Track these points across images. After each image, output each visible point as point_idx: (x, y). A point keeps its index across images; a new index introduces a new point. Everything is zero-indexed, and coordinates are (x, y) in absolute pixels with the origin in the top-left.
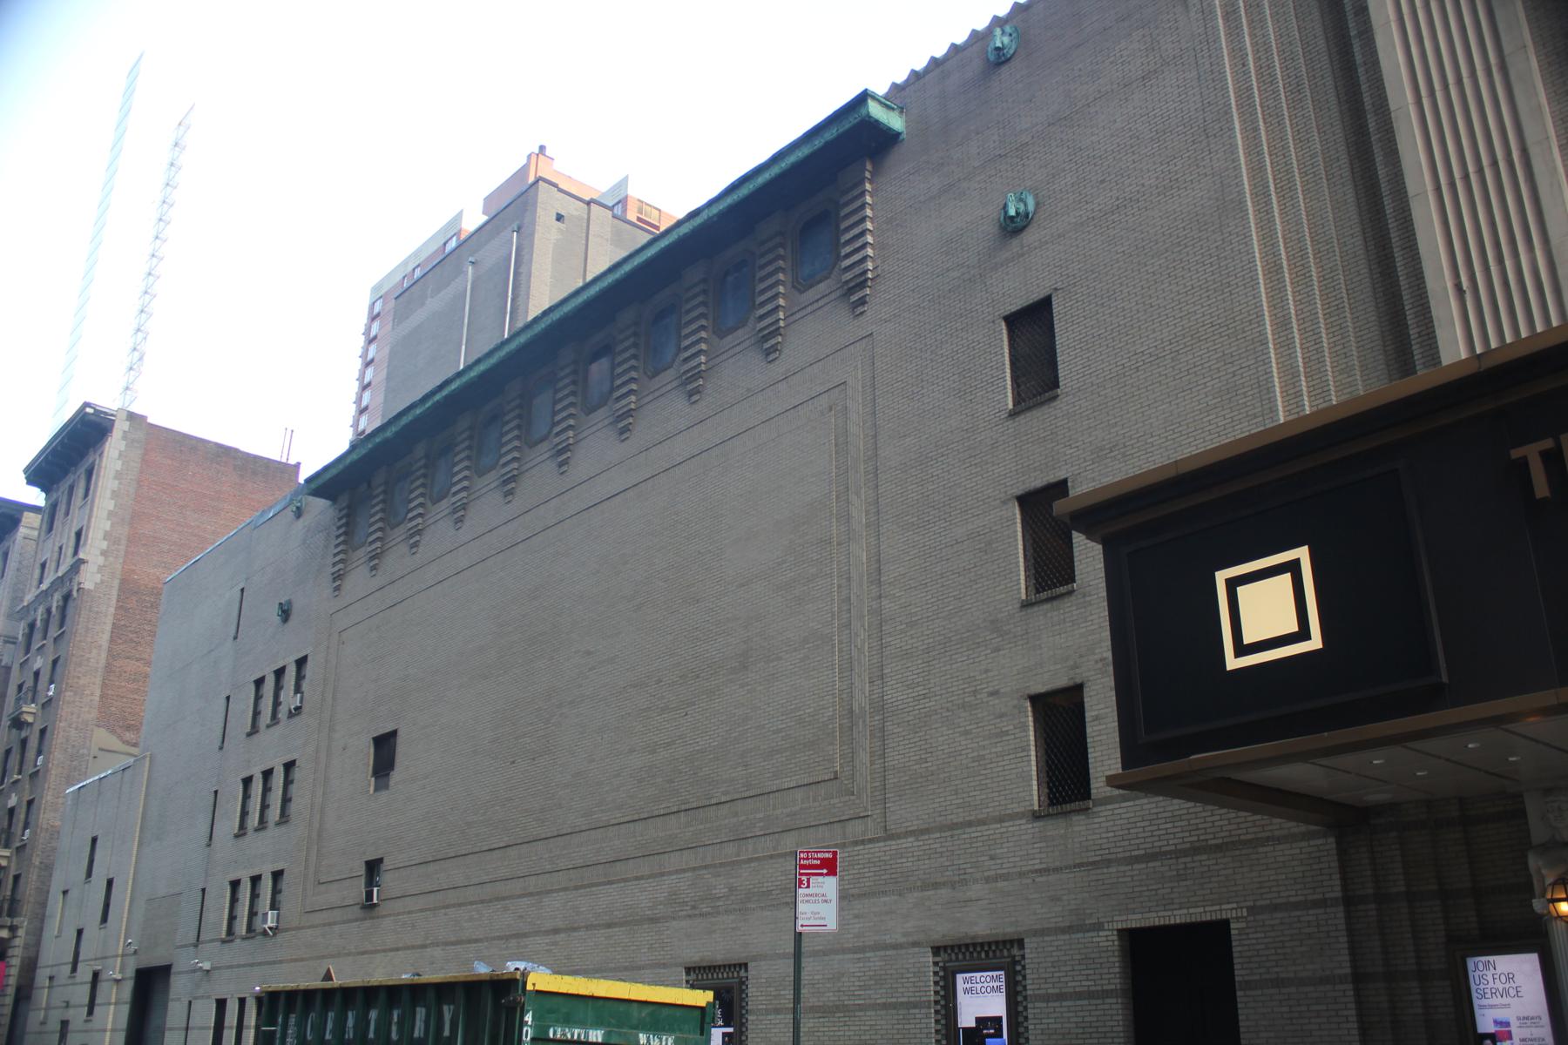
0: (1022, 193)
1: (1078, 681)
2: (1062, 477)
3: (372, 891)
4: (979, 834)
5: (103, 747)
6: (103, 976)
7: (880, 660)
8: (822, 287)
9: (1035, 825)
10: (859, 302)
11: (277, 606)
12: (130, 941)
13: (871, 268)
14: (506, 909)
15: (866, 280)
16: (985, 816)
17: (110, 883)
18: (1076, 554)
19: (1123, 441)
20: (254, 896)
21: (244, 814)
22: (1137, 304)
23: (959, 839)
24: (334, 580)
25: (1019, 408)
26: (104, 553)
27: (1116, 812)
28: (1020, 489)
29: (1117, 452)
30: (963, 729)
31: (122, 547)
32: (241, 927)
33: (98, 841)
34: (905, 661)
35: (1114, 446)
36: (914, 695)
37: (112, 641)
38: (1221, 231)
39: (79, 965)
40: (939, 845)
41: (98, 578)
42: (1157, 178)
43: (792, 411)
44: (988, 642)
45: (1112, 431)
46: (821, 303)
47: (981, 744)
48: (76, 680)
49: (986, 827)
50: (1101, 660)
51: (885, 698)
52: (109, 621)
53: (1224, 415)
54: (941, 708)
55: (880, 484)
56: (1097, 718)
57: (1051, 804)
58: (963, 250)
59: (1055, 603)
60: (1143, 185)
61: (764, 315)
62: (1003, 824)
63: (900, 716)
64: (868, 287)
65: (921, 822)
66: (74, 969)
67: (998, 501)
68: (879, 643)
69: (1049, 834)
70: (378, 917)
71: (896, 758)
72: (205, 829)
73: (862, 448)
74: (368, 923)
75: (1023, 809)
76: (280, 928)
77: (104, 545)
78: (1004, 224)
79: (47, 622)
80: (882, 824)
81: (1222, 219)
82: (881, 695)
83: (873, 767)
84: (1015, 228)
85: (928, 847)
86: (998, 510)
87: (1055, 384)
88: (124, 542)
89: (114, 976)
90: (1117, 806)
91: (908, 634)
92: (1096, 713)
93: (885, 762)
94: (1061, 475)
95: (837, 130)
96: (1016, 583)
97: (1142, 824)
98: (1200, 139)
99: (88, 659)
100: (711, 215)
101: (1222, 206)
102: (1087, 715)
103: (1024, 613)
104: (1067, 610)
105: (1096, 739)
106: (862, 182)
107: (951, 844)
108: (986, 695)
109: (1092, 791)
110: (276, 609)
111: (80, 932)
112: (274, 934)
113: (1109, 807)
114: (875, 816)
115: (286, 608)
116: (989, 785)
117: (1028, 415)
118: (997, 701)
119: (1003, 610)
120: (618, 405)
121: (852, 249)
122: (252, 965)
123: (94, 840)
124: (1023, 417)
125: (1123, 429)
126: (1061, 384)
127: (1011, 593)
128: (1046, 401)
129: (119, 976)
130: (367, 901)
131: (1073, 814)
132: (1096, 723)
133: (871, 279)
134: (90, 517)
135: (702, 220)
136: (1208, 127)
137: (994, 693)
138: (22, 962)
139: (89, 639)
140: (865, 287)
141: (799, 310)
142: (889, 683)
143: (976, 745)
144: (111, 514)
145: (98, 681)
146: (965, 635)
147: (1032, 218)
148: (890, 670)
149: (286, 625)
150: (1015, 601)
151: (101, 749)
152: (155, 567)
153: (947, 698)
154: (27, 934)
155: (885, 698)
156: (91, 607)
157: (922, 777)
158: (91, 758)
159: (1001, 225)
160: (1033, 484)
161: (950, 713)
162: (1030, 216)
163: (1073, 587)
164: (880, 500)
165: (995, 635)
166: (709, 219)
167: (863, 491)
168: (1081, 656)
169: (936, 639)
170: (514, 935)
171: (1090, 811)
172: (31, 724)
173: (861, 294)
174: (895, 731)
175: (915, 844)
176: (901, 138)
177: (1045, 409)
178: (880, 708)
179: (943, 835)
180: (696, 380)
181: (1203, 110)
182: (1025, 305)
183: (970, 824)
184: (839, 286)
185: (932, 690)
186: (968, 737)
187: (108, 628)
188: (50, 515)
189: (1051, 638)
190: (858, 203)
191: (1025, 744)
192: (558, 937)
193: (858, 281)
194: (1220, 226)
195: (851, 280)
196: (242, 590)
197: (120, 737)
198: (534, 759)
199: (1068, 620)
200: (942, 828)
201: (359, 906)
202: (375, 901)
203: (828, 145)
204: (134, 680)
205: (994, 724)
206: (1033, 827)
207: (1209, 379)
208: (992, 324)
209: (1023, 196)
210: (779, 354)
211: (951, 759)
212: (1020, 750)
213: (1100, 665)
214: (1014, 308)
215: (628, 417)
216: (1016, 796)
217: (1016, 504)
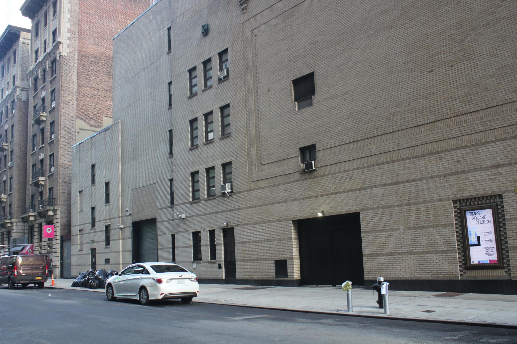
3: (312, 162)
5: (81, 128)
6: (113, 227)
11: (201, 28)
12: (127, 209)
14: (441, 159)
17: (107, 184)
20: (210, 178)
21: (193, 138)
24: (241, 5)
26: (69, 39)
31: (77, 36)
32: (203, 193)
33: (96, 166)
37: (78, 79)
39: (96, 223)
41: (68, 50)
48: (65, 98)
52: (76, 70)
66: (93, 225)
70: (317, 177)
72: (167, 149)
74: (309, 181)
76: (235, 190)
77: (69, 35)
79: (44, 76)
88: (77, 33)
89: (120, 226)
99: (69, 88)
110: (200, 30)
111: (93, 209)
112: (231, 196)
115: (206, 28)
122: (216, 213)
123: (93, 166)
129: (122, 226)
130: (307, 168)
134: (60, 24)
138: (61, 225)
139: (68, 79)
144: (70, 20)
145: (75, 98)
149: (207, 37)
151: (80, 129)
152: (92, 44)
154: (61, 212)
156: (67, 64)
158: (77, 133)
170: (452, 173)
172: (45, 121)
187: (76, 73)
188: (36, 31)
192: (500, 170)
196: (169, 29)
197: (87, 123)
198: (452, 66)
201: (298, 173)
202: (314, 168)
204: (90, 97)
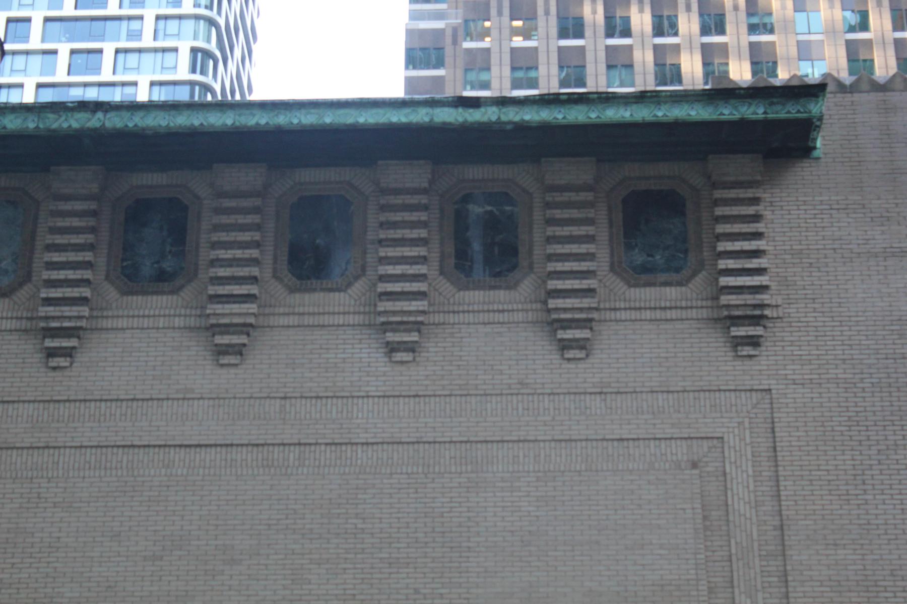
8: (672, 293)
15: (762, 317)
43: (616, 443)
46: (669, 314)
61: (561, 291)
64: (765, 327)
95: (765, 113)
100: (504, 118)
120: (219, 308)
135: (485, 119)
140: (758, 325)
141: (625, 309)
166: (499, 122)
167: (760, 595)
176: (816, 153)
180: (409, 331)
184: (704, 303)
193: (749, 313)
195: (737, 306)
203: (743, 123)
210: (587, 356)
215: (242, 333)
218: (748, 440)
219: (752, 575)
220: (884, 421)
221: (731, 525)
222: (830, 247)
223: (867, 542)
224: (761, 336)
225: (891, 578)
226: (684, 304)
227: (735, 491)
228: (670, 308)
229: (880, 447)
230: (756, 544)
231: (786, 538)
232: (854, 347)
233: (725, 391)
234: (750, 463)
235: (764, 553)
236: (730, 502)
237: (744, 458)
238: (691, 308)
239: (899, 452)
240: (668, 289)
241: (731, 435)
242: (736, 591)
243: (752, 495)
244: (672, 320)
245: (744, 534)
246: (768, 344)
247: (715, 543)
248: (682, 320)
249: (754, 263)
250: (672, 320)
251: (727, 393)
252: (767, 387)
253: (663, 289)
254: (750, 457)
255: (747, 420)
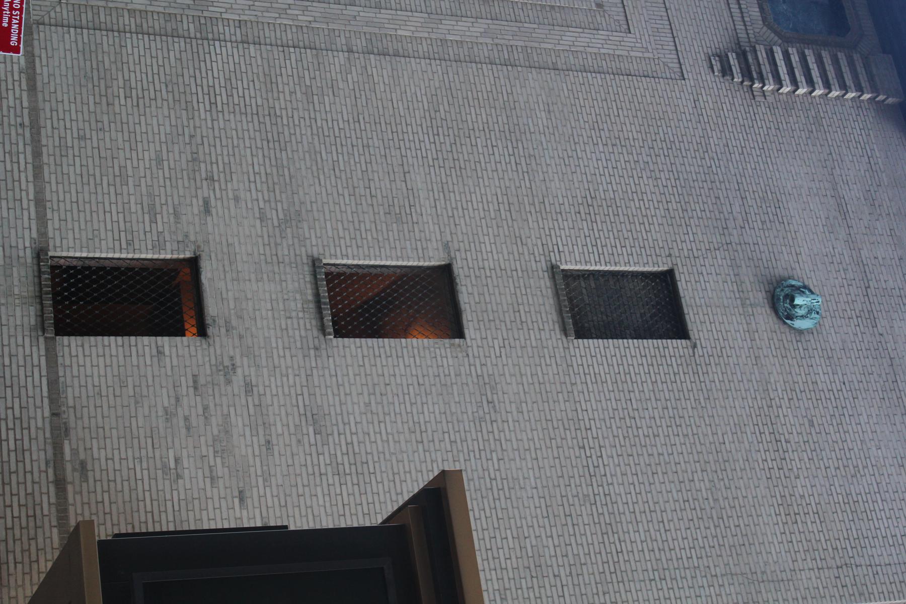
0: (818, 313)
1: (210, 331)
2: (466, 332)
4: (22, 168)
7: (268, 41)
9: (28, 251)
10: (726, 66)
13: (765, 88)
15: (752, 80)
16: (47, 179)
18: (369, 340)
19: (499, 420)
22: (659, 454)
23: (17, 134)
25: (559, 277)
27: (36, 370)
28: (459, 270)
29: (486, 410)
30: (165, 158)
34: (262, 79)
35: (494, 407)
36: (217, 86)
38: (726, 574)
40: (12, 104)
42: (802, 497)
44: (273, 205)
45: (513, 405)
47: (143, 180)
49: (31, 179)
50: (233, 365)
51: (217, 43)
53: (510, 558)
54: (195, 127)
55: (494, 66)
56: (160, 353)
57: (53, 268)
58: (763, 222)
59: (312, 305)
60: (797, 477)
62: (32, 204)
63: (190, 63)
64: (742, 82)
65: (46, 81)
67: (449, 239)
68: (290, 43)
69: (15, 269)
71: (136, 50)
73: (543, 46)
75: (51, 235)
78: (785, 284)
80: (47, 21)
81: (740, 577)
82: (222, 37)
83: (126, 14)
84: (779, 299)
85: (10, 87)
86: (439, 238)
87: (581, 334)
90: (44, 373)
91: (297, 88)
92: (167, 353)
93: (131, 32)
94: (470, 330)
96: (344, 252)
97: (17, 406)
98: (837, 558)
101: (755, 578)
102: (166, 339)
103: (305, 261)
104: (301, 322)
105: (134, 349)
106: (875, 90)
107: (13, 122)
108: (206, 195)
109: (66, 339)
113: (43, 359)
114: (58, 9)
116: (86, 188)
117: (549, 291)
118: (196, 211)
119: (312, 231)
121: (794, 65)
124: (548, 284)
125: (514, 421)
126: (580, 341)
127: (332, 244)
128: (563, 318)
131: (38, 307)
132: (154, 352)
133: (751, 86)
136: (850, 569)
137: (207, 209)
140: (743, 76)
142: (235, 50)
143: (142, 174)
146: (286, 170)
147: (785, 323)
148: (253, 54)
150: (321, 251)
153: (207, 137)
155: (217, 43)
157: (106, 87)
159: (784, 279)
160: (463, 289)
161: (187, 141)
162: (788, 321)
163: (330, 334)
164: (474, 65)
165: (281, 216)
167: (489, 41)
168: (241, 337)
169: (286, 128)
171: (40, 333)
173: (736, 69)
174: (172, 53)
175: (16, 67)
177: (554, 316)
178: (204, 35)
179: (26, 112)
181: (871, 565)
182: (683, 300)
183: (37, 154)
185: (220, 115)
186: (154, 163)
189: (267, 296)
190: (849, 82)
191: (137, 247)
193: (753, 68)
194: (732, 574)
199: (289, 321)
200: (34, 112)
205: (166, 204)
206: (25, 248)
207: (556, 543)
208: (667, 253)
209: (813, 315)
211: (126, 134)
212: (129, 238)
213: (227, 362)
214: (682, 286)
216: (70, 226)
217: (443, 263)
218: (632, 54)
219: (506, 37)
220: (678, 172)
221: (551, 27)
222: (833, 151)
223: (557, 139)
224: (733, 79)
225: (527, 155)
226: (746, 19)
227: (582, 35)
228: (740, 8)
229: (651, 163)
230: (536, 45)
231: (547, 71)
232: (742, 156)
233: (675, 42)
234: (611, 52)
235: (529, 51)
236: (571, 29)
237: (615, 47)
238: (745, 25)
239: (650, 180)
240: (757, 10)
241: (634, 40)
242: (490, 22)
243: (582, 49)
244: (730, 8)
245: (544, 36)
246: (727, 84)
247: (530, 12)
248: (732, 17)
249: (800, 77)
250: (730, 8)
251: (672, 44)
252: (686, 76)
253: (757, 6)
254: (617, 52)
255: (651, 55)
